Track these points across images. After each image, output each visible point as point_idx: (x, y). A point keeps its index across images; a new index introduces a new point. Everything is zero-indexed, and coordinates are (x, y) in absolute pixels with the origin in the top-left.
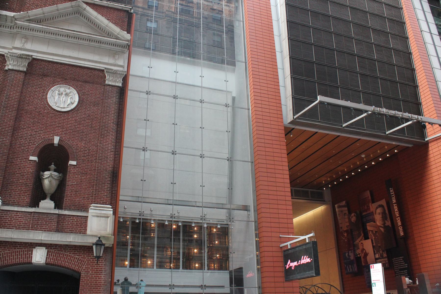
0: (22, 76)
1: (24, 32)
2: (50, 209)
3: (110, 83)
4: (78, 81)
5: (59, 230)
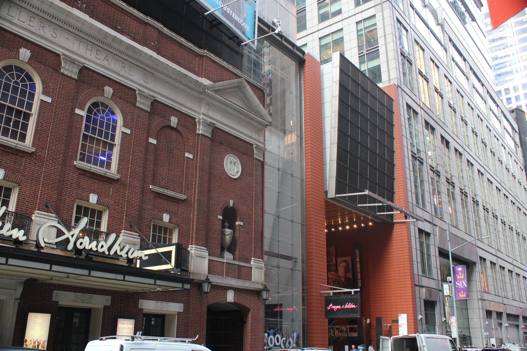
0: (208, 142)
1: (208, 99)
2: (230, 260)
3: (257, 157)
4: (239, 152)
5: (239, 277)
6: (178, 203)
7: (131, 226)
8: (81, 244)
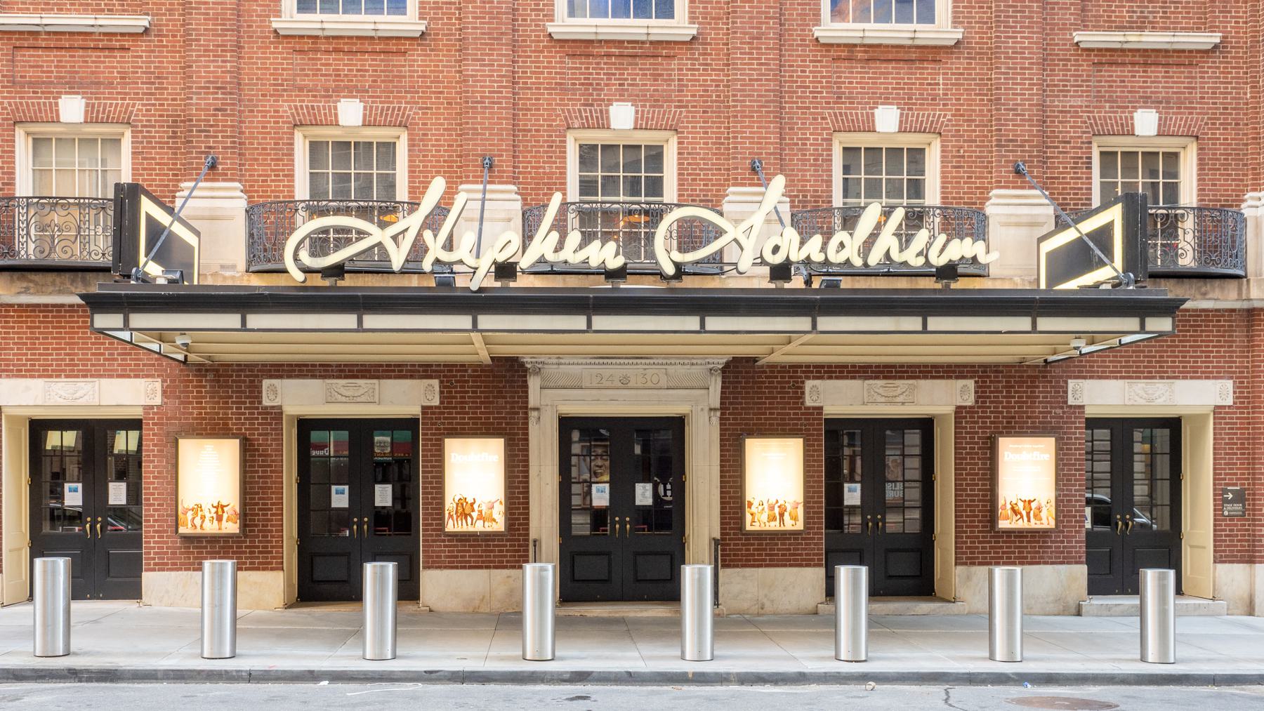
6: (1191, 65)
7: (1018, 172)
8: (776, 249)
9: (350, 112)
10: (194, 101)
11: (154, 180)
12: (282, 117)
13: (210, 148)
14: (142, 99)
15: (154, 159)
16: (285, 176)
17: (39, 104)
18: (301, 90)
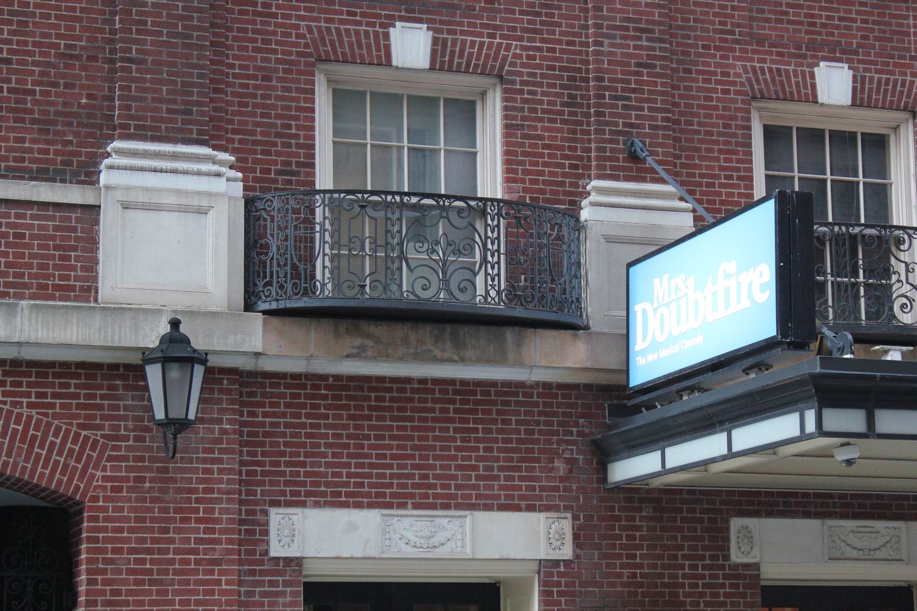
9: (834, 83)
10: (605, 49)
11: (542, 173)
12: (734, 83)
13: (632, 125)
14: (520, 39)
15: (541, 137)
16: (740, 178)
17: (357, 33)
18: (760, 43)
